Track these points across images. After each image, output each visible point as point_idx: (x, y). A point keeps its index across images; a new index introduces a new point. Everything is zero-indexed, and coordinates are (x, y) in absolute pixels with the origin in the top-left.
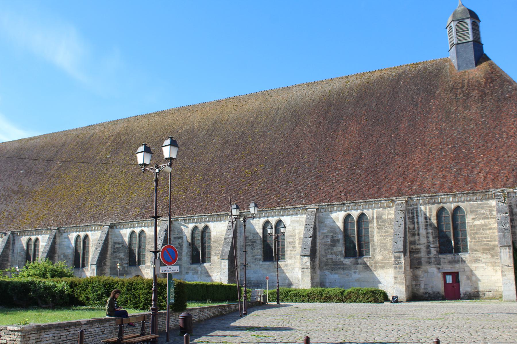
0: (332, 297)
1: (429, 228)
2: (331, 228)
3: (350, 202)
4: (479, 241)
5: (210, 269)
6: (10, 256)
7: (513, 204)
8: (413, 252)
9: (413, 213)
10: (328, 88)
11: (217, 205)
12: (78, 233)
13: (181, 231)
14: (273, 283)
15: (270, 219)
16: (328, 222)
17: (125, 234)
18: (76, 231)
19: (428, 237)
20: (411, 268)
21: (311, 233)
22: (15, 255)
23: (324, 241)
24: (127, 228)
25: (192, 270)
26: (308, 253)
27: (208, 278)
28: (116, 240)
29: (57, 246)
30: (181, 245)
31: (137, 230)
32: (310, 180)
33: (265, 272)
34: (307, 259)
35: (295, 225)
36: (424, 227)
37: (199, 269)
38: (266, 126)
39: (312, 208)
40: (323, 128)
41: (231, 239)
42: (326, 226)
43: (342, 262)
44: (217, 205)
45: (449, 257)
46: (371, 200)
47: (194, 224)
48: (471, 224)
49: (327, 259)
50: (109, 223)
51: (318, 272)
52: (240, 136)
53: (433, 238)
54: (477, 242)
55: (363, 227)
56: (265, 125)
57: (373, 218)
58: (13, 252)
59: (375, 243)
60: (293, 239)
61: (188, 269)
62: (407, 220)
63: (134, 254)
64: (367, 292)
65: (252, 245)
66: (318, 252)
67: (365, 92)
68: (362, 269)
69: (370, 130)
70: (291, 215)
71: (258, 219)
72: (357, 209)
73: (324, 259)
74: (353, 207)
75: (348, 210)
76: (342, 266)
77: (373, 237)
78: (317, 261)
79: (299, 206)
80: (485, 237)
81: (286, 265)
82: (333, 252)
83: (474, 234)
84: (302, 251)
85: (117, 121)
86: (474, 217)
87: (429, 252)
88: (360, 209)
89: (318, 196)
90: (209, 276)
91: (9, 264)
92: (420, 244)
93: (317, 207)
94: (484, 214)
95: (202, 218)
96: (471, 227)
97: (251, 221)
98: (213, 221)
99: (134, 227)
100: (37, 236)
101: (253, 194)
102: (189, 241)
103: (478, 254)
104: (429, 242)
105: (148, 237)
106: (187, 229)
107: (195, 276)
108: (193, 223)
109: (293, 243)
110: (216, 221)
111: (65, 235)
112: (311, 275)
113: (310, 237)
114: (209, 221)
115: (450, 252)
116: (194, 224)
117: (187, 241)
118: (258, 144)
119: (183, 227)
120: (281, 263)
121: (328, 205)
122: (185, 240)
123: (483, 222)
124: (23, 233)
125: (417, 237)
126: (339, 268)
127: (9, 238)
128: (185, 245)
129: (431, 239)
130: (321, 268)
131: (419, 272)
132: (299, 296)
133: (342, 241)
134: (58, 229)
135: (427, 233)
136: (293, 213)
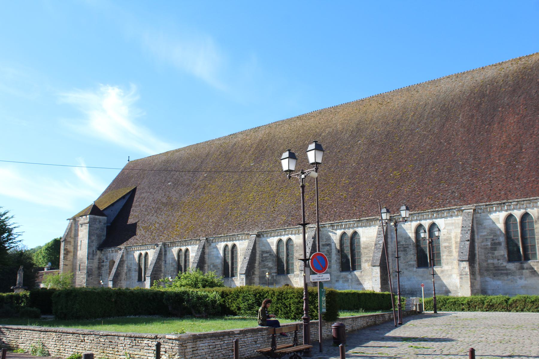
0: (496, 306)
2: (491, 230)
3: (510, 201)
5: (361, 276)
6: (163, 266)
10: (479, 78)
11: (366, 210)
12: (225, 243)
13: (329, 238)
14: (429, 290)
15: (423, 222)
16: (486, 223)
17: (273, 243)
18: (224, 241)
21: (468, 236)
22: (167, 266)
23: (483, 244)
24: (274, 236)
25: (342, 278)
26: (467, 258)
27: (359, 286)
28: (264, 249)
29: (206, 256)
30: (329, 252)
31: (285, 238)
32: (465, 178)
33: (420, 279)
34: (465, 265)
35: (451, 228)
37: (350, 277)
38: (413, 123)
39: (469, 209)
40: (477, 122)
41: (382, 245)
42: (485, 228)
43: (505, 267)
44: (366, 210)
46: (535, 198)
47: (342, 231)
49: (488, 264)
50: (256, 232)
51: (478, 278)
52: (386, 135)
55: (527, 228)
56: (412, 123)
58: (165, 263)
60: (449, 243)
61: (338, 277)
63: (282, 262)
64: (536, 300)
65: (405, 251)
66: (477, 256)
67: (522, 78)
68: (528, 274)
69: (530, 120)
70: (446, 217)
71: (409, 223)
72: (520, 208)
73: (485, 264)
74: (515, 206)
75: (510, 210)
76: (505, 272)
78: (477, 267)
79: (453, 207)
81: (442, 272)
82: (494, 256)
84: (459, 256)
85: (259, 128)
88: (523, 208)
90: (360, 284)
91: (162, 274)
93: (474, 208)
95: (350, 224)
97: (403, 225)
98: (361, 227)
99: (281, 235)
100: (235, 242)
101: (404, 197)
102: (338, 247)
105: (295, 245)
106: (335, 236)
107: (346, 284)
108: (341, 229)
109: (449, 247)
110: (366, 226)
111: (213, 245)
112: (471, 282)
113: (468, 241)
114: (357, 227)
116: (342, 231)
117: (336, 248)
118: (406, 143)
119: (331, 234)
120: (437, 269)
121: (486, 205)
122: (333, 247)
124: (173, 244)
126: (502, 274)
127: (161, 249)
128: (334, 252)
130: (481, 274)
132: (458, 305)
133: (504, 244)
134: (207, 239)
136: (448, 215)
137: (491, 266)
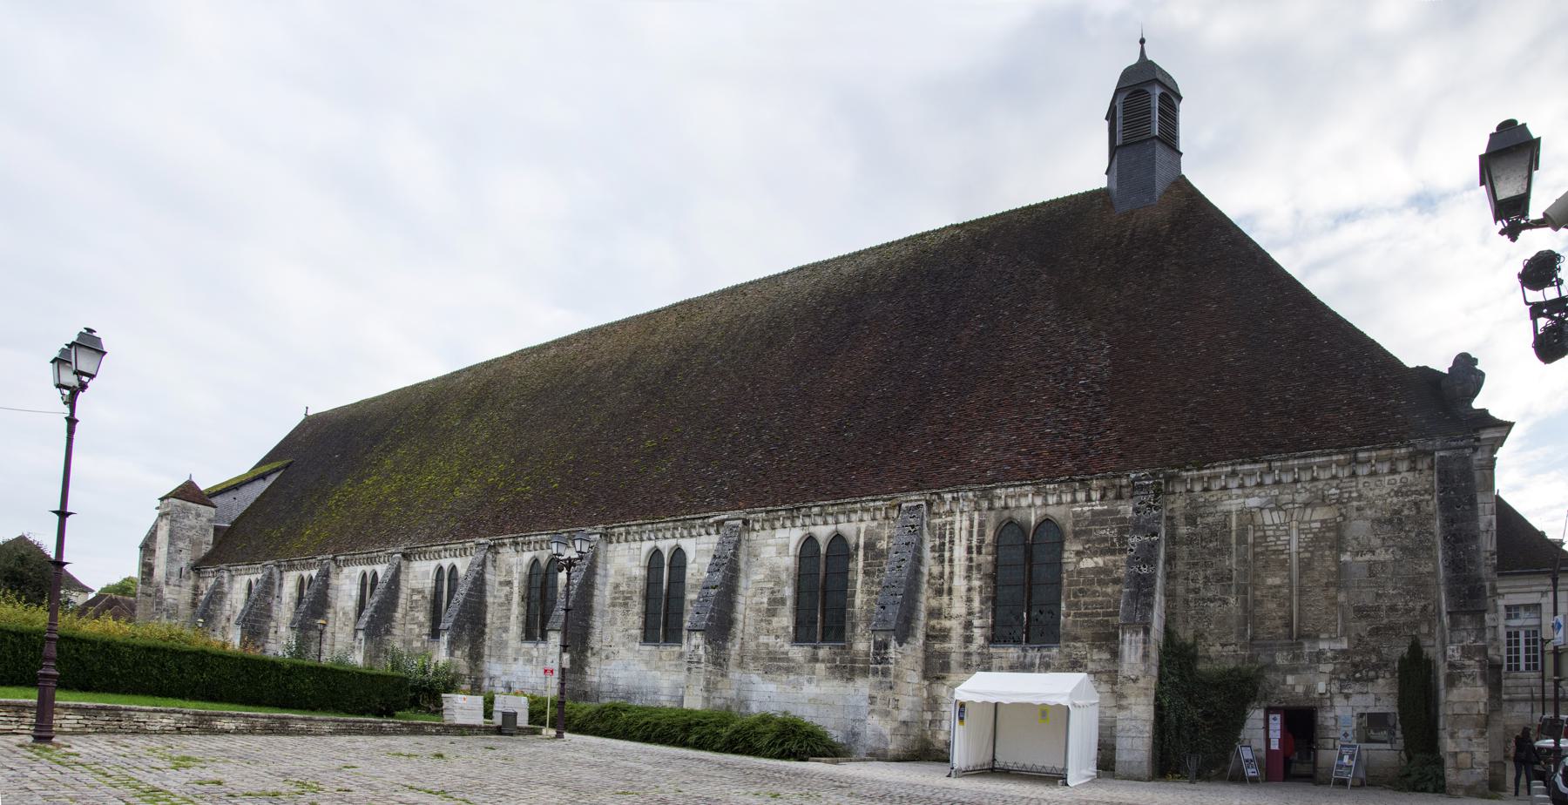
1: (975, 575)
4: (1086, 615)
7: (1177, 514)
8: (935, 637)
9: (942, 536)
19: (969, 600)
20: (925, 677)
23: (755, 600)
36: (964, 573)
45: (1013, 652)
48: (1071, 568)
50: (402, 548)
51: (735, 674)
53: (982, 603)
54: (1081, 615)
57: (857, 546)
59: (857, 610)
62: (928, 555)
65: (626, 604)
66: (740, 626)
73: (752, 645)
77: (853, 595)
78: (734, 649)
80: (1101, 603)
83: (1075, 596)
86: (1080, 548)
87: (968, 639)
89: (754, 492)
92: (950, 617)
94: (1105, 540)
96: (1070, 574)
103: (1080, 649)
104: (970, 614)
107: (528, 668)
115: (1017, 642)
123: (1100, 561)
125: (945, 598)
126: (779, 668)
129: (976, 604)
131: (942, 690)
133: (789, 603)
135: (969, 590)
137: (763, 650)
